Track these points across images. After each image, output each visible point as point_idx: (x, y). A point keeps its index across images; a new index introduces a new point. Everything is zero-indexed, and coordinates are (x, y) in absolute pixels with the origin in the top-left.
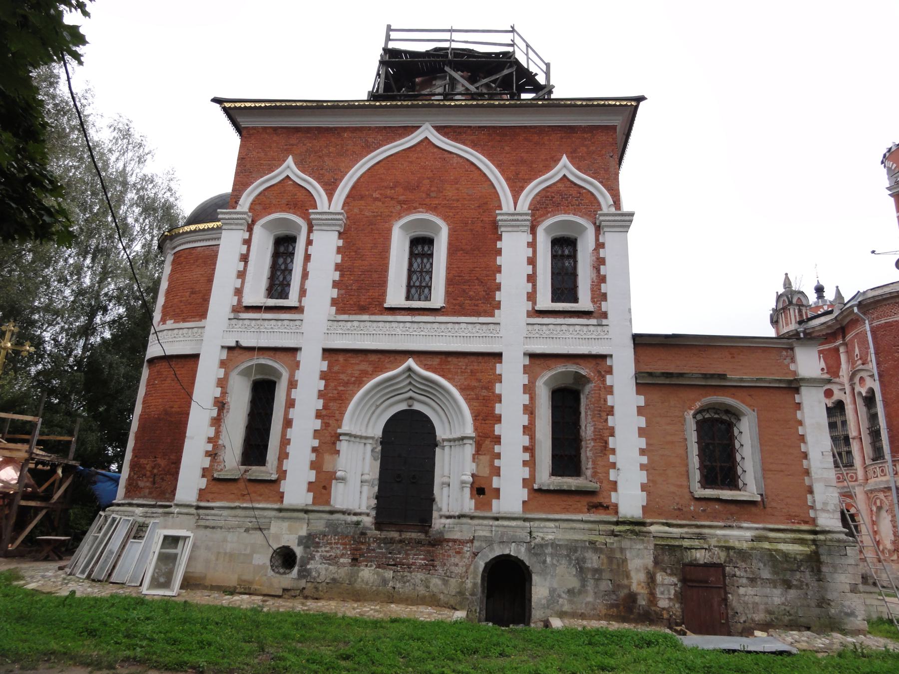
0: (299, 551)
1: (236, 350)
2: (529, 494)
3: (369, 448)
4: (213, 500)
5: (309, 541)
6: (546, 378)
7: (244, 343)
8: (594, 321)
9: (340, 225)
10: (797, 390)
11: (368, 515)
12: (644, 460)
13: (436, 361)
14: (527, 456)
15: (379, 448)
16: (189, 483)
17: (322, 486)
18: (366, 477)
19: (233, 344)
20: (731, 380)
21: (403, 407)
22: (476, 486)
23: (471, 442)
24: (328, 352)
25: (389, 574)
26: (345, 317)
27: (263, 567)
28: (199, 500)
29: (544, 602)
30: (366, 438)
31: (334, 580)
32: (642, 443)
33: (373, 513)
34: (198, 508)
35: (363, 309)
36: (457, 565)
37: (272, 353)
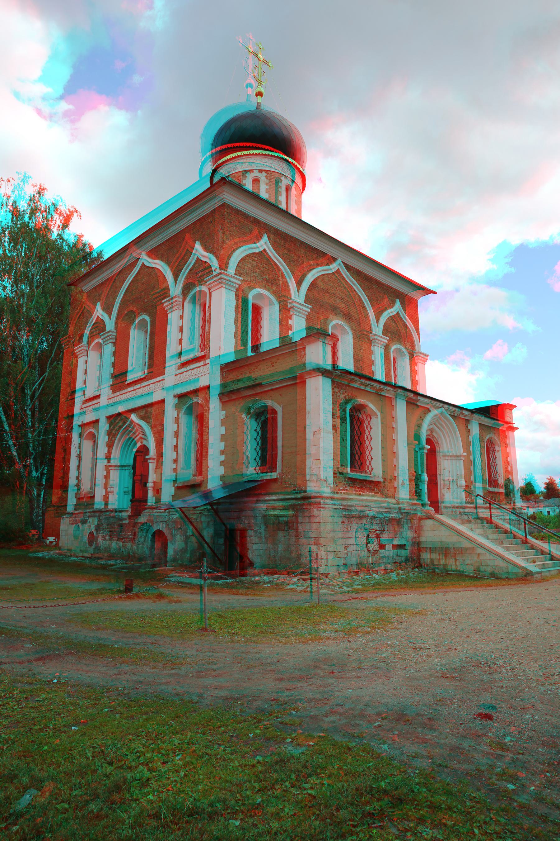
0: (95, 533)
1: (83, 426)
2: (175, 490)
3: (127, 472)
4: (79, 509)
5: (98, 528)
6: (183, 411)
7: (85, 422)
8: (202, 363)
9: (112, 338)
10: (304, 383)
11: (127, 511)
12: (223, 458)
13: (142, 413)
14: (174, 466)
15: (132, 471)
16: (72, 501)
17: (106, 498)
18: (126, 489)
19: (80, 423)
20: (266, 385)
21: (139, 444)
22: (156, 489)
23: (153, 461)
24: (109, 418)
25: (121, 544)
26: (118, 393)
27: (85, 543)
28: (75, 509)
29: (172, 557)
30: (125, 466)
31: (105, 548)
32: (222, 446)
33: (130, 510)
34: (73, 514)
35: (120, 389)
36: (141, 537)
37: (92, 425)
